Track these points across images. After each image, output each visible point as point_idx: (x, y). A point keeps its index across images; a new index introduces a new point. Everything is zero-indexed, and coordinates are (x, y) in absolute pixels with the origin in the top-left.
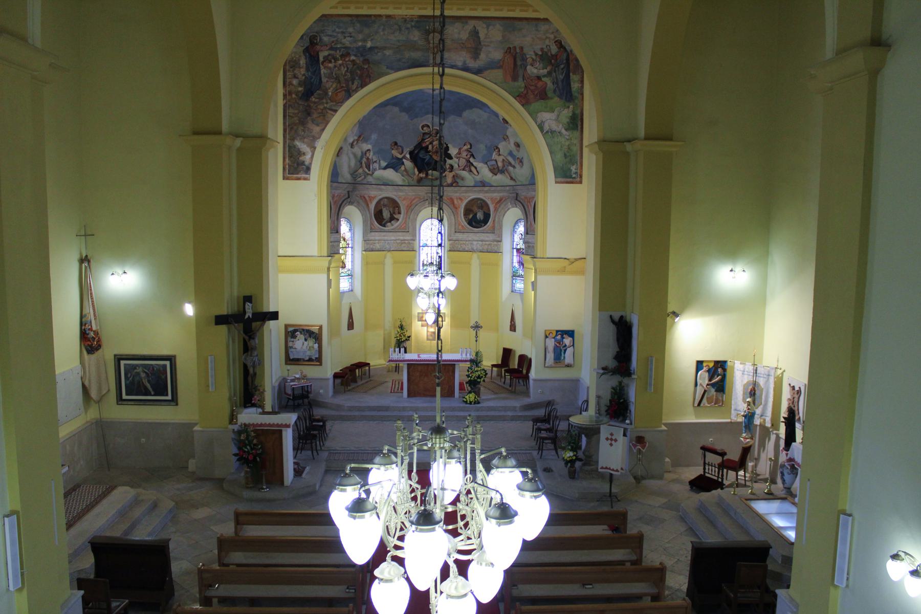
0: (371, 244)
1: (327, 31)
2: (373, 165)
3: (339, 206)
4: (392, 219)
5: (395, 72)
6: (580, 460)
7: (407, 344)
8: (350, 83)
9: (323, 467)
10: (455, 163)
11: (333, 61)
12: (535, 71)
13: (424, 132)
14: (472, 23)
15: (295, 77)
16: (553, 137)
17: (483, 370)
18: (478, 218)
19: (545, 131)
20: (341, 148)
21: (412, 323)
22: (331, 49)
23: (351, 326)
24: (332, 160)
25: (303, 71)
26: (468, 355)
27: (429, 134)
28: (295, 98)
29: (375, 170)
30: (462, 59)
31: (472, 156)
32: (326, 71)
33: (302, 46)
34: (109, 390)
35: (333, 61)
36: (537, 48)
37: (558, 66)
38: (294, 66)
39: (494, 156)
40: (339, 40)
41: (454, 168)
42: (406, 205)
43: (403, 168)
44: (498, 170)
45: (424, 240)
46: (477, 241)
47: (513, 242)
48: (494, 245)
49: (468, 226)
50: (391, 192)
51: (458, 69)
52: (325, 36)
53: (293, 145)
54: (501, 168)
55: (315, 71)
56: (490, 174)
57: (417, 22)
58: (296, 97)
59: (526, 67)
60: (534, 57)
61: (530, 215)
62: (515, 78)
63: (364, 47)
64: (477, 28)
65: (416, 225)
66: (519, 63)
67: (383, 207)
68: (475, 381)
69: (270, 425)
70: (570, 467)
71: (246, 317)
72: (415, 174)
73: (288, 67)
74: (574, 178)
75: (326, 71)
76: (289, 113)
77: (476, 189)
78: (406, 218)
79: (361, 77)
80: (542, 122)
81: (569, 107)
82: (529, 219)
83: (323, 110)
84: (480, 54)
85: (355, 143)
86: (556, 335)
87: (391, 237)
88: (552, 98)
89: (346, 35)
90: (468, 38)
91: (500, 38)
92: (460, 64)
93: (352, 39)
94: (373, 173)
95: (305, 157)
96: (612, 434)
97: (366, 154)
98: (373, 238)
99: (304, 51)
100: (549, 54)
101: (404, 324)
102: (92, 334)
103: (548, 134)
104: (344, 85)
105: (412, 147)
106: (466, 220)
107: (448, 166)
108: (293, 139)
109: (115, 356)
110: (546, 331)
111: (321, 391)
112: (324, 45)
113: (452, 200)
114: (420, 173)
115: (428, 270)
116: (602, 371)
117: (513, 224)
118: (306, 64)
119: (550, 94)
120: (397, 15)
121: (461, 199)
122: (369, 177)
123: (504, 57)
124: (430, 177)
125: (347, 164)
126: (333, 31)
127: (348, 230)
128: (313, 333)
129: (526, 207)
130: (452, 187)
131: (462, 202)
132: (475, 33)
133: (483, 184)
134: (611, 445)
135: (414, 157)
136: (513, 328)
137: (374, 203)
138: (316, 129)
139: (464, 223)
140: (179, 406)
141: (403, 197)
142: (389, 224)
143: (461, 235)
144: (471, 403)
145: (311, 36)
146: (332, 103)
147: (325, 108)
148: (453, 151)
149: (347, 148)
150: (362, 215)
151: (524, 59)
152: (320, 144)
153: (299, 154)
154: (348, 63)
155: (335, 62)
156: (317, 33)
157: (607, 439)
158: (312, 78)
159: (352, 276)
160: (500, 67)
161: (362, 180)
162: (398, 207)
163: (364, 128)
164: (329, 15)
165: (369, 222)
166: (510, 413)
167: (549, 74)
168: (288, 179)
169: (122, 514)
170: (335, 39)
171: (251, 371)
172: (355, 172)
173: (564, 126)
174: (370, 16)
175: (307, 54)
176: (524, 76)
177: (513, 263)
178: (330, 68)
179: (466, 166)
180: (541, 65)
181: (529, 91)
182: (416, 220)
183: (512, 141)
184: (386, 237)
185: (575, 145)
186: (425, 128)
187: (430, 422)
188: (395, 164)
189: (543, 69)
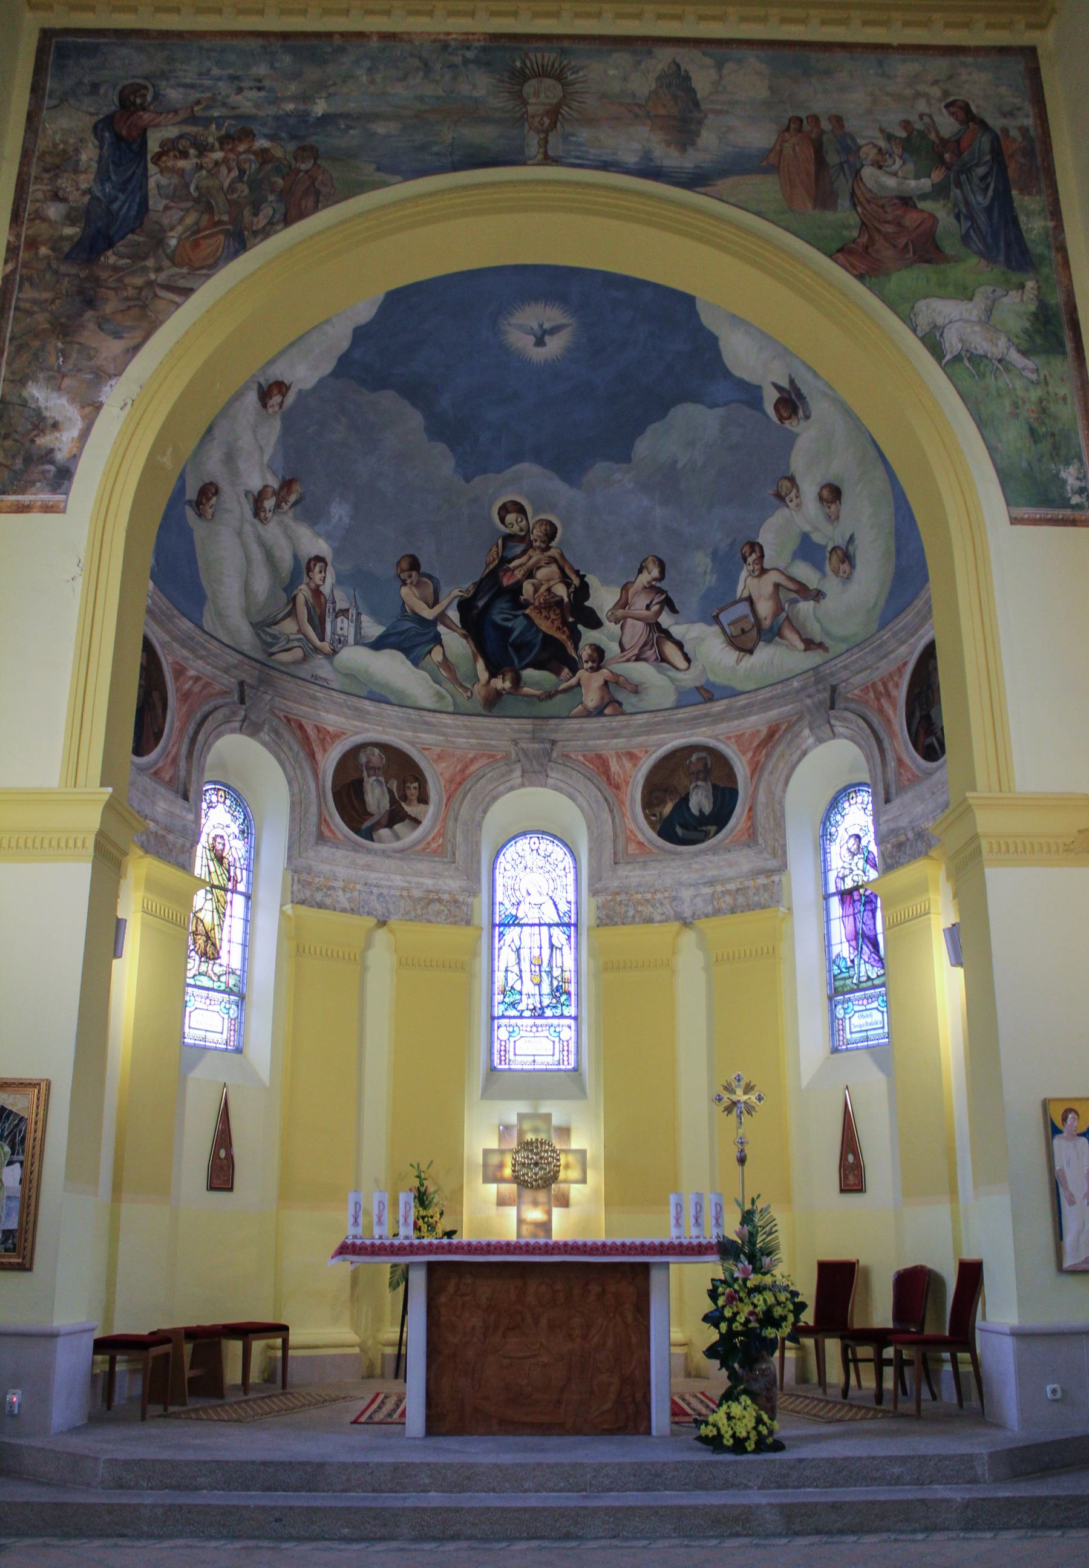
0: (319, 889)
1: (180, 74)
2: (334, 622)
3: (198, 716)
4: (395, 816)
5: (407, 179)
8: (247, 213)
10: (611, 638)
11: (192, 151)
12: (891, 182)
13: (508, 531)
14: (664, 56)
15: (56, 196)
16: (982, 376)
18: (695, 811)
19: (948, 357)
21: (457, 1194)
22: (192, 119)
25: (86, 181)
27: (523, 539)
28: (47, 257)
29: (342, 642)
30: (636, 146)
31: (668, 604)
32: (164, 181)
33: (91, 114)
35: (192, 151)
36: (892, 118)
37: (967, 170)
38: (58, 167)
39: (746, 583)
40: (219, 98)
41: (608, 655)
42: (447, 776)
43: (437, 655)
44: (759, 632)
45: (508, 905)
46: (695, 885)
47: (826, 872)
48: (758, 889)
49: (661, 842)
50: (395, 727)
52: (172, 87)
53: (20, 395)
54: (767, 624)
55: (130, 179)
56: (732, 655)
57: (484, 49)
58: (51, 253)
60: (882, 144)
61: (892, 734)
62: (824, 199)
63: (303, 117)
64: (683, 68)
65: (478, 843)
66: (833, 158)
67: (365, 774)
68: (747, 1332)
73: (34, 171)
74: (1078, 507)
75: (164, 181)
76: (18, 299)
77: (682, 714)
78: (444, 819)
79: (284, 195)
80: (935, 326)
81: (1022, 286)
82: (890, 755)
83: (140, 289)
84: (698, 134)
85: (269, 503)
88: (957, 260)
89: (242, 85)
90: (655, 92)
91: (763, 93)
92: (631, 159)
93: (262, 94)
94: (335, 652)
95: (57, 435)
97: (309, 570)
98: (326, 868)
99: (95, 127)
100: (933, 136)
104: (225, 218)
105: (463, 587)
106: (652, 824)
107: (585, 652)
108: (19, 380)
112: (168, 112)
113: (601, 764)
114: (493, 675)
115: (521, 1007)
118: (99, 162)
119: (950, 247)
120: (415, 33)
121: (632, 756)
122: (320, 660)
123: (781, 140)
124: (526, 690)
126: (200, 74)
127: (235, 829)
129: (875, 720)
130: (603, 719)
131: (635, 766)
133: (707, 693)
138: (114, 347)
139: (644, 834)
141: (438, 749)
142: (384, 832)
143: (638, 872)
144: (739, 1446)
145: (125, 87)
146: (175, 270)
147: (151, 284)
150: (290, 782)
151: (849, 147)
153: (36, 427)
154: (243, 156)
155: (201, 155)
156: (146, 78)
158: (116, 199)
159: (242, 997)
161: (294, 663)
162: (416, 780)
164: (191, 33)
165: (314, 809)
167: (940, 191)
170: (208, 95)
172: (269, 625)
173: (1016, 340)
174: (329, 35)
175: (107, 134)
176: (853, 194)
177: (829, 945)
178: (181, 172)
179: (645, 644)
180: (910, 166)
181: (877, 237)
182: (479, 825)
183: (809, 489)
184: (374, 875)
185: (1064, 399)
186: (511, 518)
187: (534, 1544)
189: (917, 177)
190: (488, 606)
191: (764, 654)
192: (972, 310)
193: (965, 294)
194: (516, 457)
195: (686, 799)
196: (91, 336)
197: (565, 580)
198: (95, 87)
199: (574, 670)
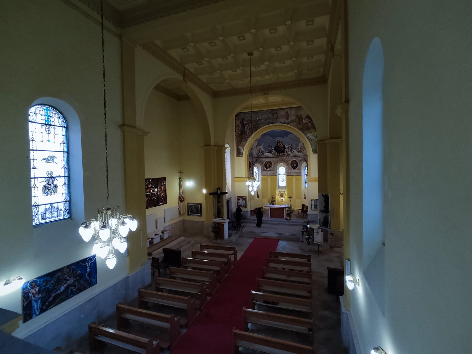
4: (270, 167)
6: (311, 239)
7: (274, 202)
8: (253, 130)
9: (238, 235)
12: (306, 122)
14: (286, 110)
15: (238, 129)
17: (292, 210)
20: (252, 148)
21: (276, 197)
22: (248, 121)
23: (258, 197)
24: (249, 151)
25: (240, 128)
26: (288, 206)
29: (264, 153)
31: (292, 148)
34: (186, 212)
39: (298, 147)
43: (272, 152)
51: (283, 123)
56: (297, 153)
59: (303, 121)
62: (299, 124)
66: (300, 120)
69: (221, 222)
70: (308, 241)
71: (218, 193)
72: (276, 154)
73: (236, 127)
77: (294, 157)
85: (257, 146)
86: (315, 200)
87: (270, 172)
96: (317, 231)
97: (261, 149)
98: (264, 172)
101: (273, 196)
102: (182, 197)
103: (310, 140)
105: (275, 146)
107: (285, 151)
109: (187, 203)
110: (311, 199)
111: (246, 215)
114: (277, 154)
116: (320, 211)
117: (305, 167)
125: (255, 152)
127: (257, 170)
128: (244, 198)
132: (287, 113)
133: (295, 156)
134: (317, 234)
135: (275, 149)
136: (305, 198)
137: (264, 162)
138: (244, 143)
140: (202, 217)
142: (269, 168)
144: (288, 220)
147: (246, 137)
148: (287, 147)
149: (254, 148)
152: (245, 147)
155: (249, 124)
157: (316, 232)
160: (295, 121)
161: (261, 156)
163: (259, 142)
166: (299, 224)
167: (310, 122)
168: (237, 157)
169: (179, 243)
171: (219, 208)
188: (270, 152)
189: (308, 121)
190: (277, 148)
191: (300, 153)
192: (311, 134)
193: (311, 133)
194: (278, 136)
195: (294, 165)
196: (243, 142)
197: (283, 145)
198: (240, 118)
199: (284, 153)
